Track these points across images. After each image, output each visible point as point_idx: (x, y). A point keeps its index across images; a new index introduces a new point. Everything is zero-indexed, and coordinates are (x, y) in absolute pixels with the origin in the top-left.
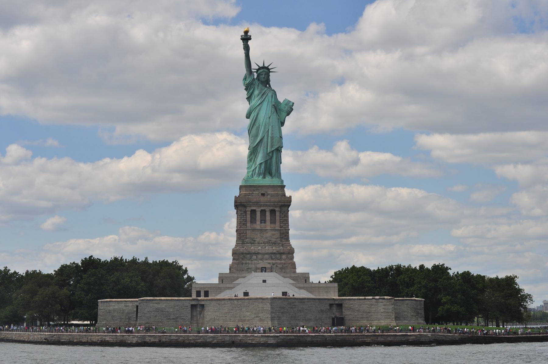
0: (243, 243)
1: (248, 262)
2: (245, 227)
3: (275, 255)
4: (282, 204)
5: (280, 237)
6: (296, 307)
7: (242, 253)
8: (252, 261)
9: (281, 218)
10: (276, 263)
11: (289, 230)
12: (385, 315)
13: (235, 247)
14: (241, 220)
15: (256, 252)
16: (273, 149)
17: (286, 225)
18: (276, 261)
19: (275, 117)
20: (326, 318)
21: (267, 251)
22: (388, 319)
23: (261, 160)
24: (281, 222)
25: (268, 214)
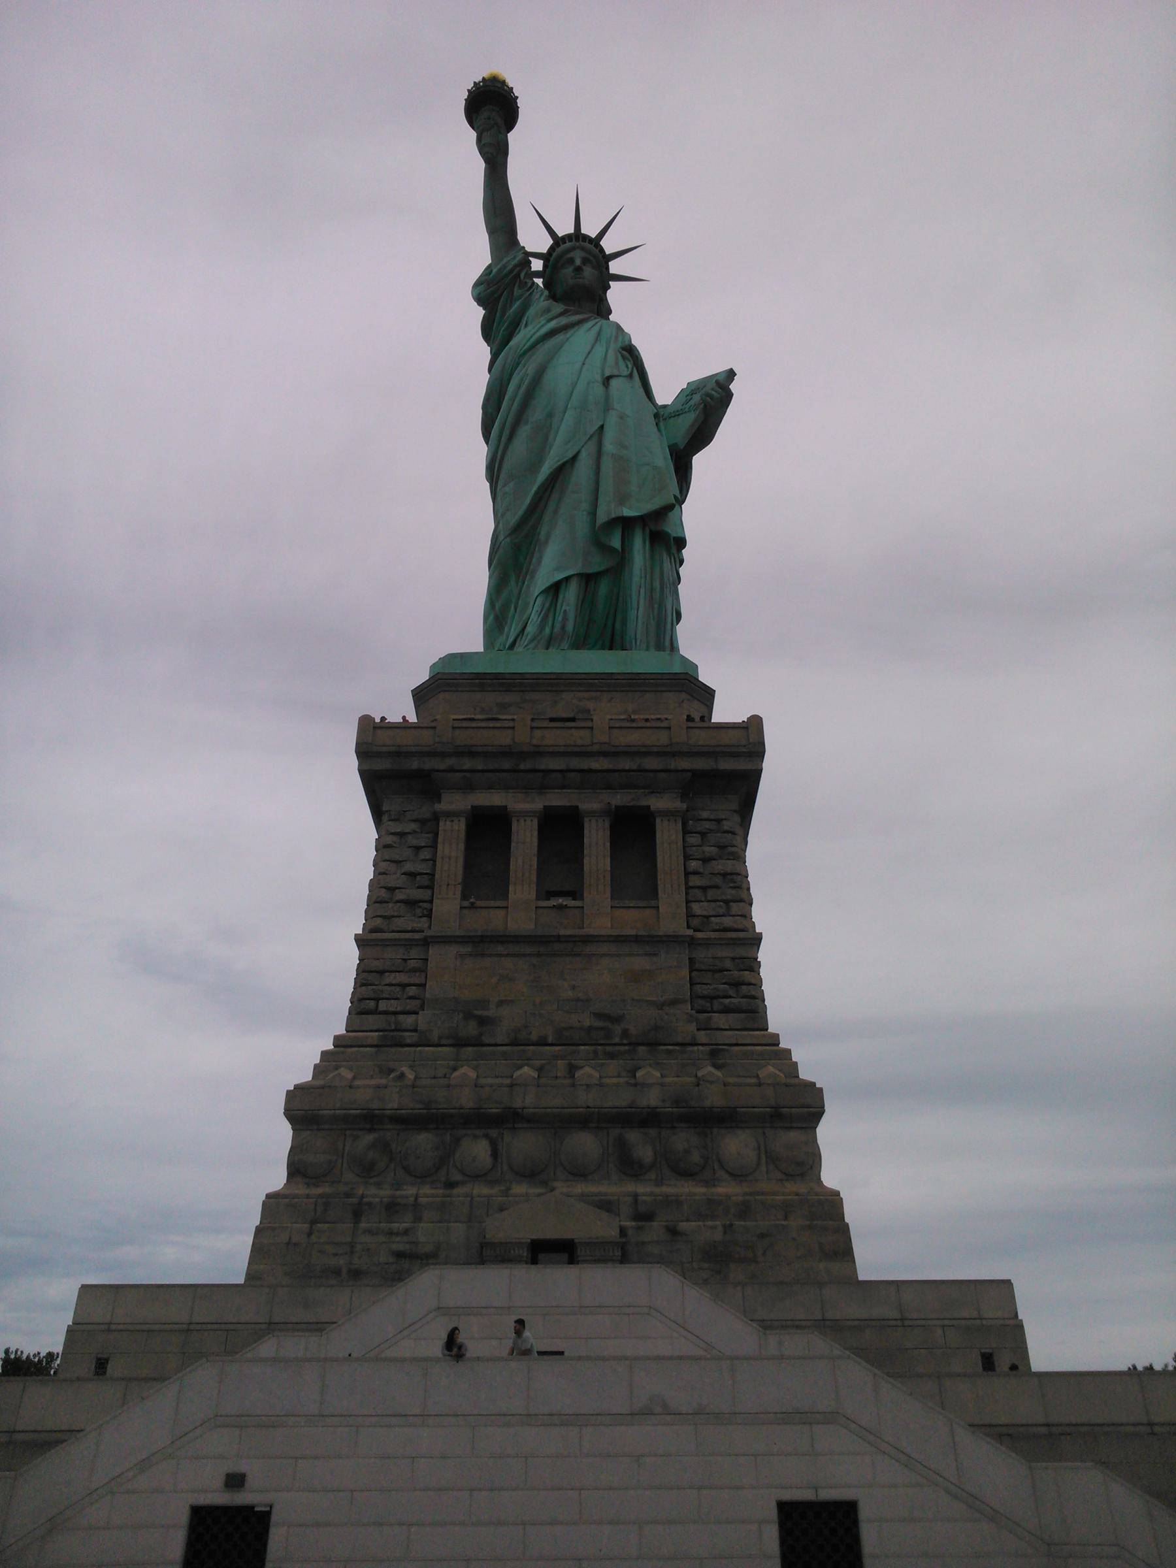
0: (391, 1040)
1: (410, 1191)
2: (423, 923)
3: (653, 1132)
4: (700, 764)
5: (694, 997)
7: (371, 1120)
8: (450, 1185)
11: (757, 940)
13: (318, 1070)
16: (627, 512)
17: (735, 909)
18: (665, 1189)
21: (586, 1099)
23: (558, 569)
24: (699, 894)
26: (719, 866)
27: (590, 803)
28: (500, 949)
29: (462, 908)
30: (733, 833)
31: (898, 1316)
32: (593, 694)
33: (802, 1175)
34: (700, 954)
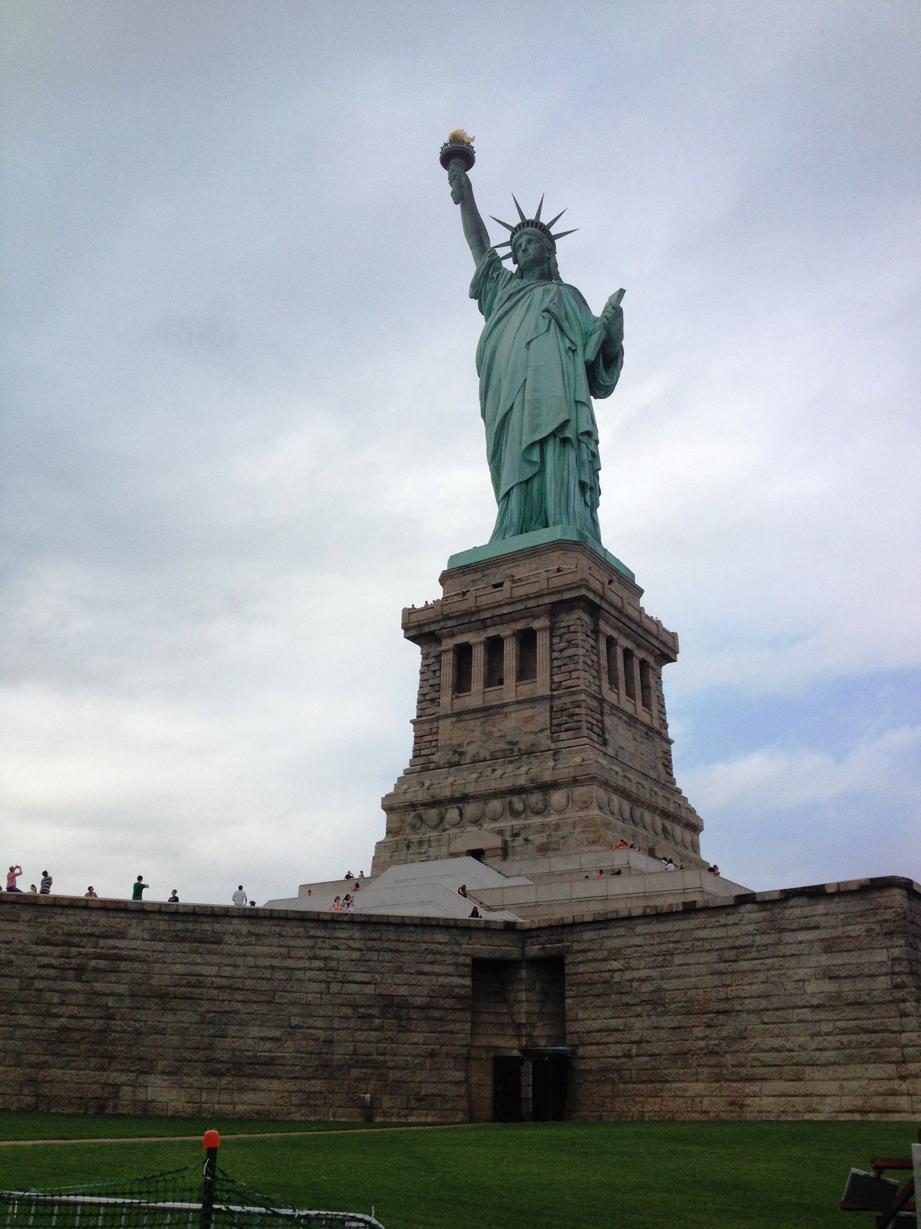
0: (425, 768)
3: (524, 796)
4: (555, 598)
5: (551, 725)
6: (123, 965)
7: (413, 806)
8: (444, 830)
9: (555, 655)
10: (525, 827)
12: (844, 1031)
14: (425, 691)
15: (458, 795)
16: (538, 437)
17: (574, 674)
18: (527, 822)
19: (551, 344)
20: (432, 1054)
22: (867, 1060)
25: (510, 650)
26: (567, 653)
27: (505, 631)
28: (468, 717)
29: (452, 699)
30: (576, 632)
31: (578, 867)
32: (516, 563)
33: (587, 807)
34: (557, 703)
